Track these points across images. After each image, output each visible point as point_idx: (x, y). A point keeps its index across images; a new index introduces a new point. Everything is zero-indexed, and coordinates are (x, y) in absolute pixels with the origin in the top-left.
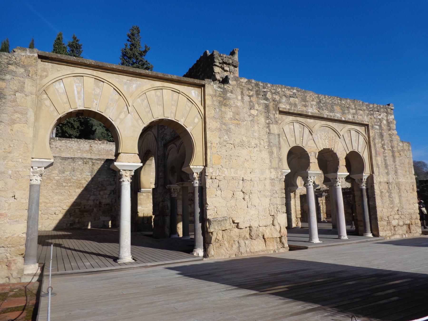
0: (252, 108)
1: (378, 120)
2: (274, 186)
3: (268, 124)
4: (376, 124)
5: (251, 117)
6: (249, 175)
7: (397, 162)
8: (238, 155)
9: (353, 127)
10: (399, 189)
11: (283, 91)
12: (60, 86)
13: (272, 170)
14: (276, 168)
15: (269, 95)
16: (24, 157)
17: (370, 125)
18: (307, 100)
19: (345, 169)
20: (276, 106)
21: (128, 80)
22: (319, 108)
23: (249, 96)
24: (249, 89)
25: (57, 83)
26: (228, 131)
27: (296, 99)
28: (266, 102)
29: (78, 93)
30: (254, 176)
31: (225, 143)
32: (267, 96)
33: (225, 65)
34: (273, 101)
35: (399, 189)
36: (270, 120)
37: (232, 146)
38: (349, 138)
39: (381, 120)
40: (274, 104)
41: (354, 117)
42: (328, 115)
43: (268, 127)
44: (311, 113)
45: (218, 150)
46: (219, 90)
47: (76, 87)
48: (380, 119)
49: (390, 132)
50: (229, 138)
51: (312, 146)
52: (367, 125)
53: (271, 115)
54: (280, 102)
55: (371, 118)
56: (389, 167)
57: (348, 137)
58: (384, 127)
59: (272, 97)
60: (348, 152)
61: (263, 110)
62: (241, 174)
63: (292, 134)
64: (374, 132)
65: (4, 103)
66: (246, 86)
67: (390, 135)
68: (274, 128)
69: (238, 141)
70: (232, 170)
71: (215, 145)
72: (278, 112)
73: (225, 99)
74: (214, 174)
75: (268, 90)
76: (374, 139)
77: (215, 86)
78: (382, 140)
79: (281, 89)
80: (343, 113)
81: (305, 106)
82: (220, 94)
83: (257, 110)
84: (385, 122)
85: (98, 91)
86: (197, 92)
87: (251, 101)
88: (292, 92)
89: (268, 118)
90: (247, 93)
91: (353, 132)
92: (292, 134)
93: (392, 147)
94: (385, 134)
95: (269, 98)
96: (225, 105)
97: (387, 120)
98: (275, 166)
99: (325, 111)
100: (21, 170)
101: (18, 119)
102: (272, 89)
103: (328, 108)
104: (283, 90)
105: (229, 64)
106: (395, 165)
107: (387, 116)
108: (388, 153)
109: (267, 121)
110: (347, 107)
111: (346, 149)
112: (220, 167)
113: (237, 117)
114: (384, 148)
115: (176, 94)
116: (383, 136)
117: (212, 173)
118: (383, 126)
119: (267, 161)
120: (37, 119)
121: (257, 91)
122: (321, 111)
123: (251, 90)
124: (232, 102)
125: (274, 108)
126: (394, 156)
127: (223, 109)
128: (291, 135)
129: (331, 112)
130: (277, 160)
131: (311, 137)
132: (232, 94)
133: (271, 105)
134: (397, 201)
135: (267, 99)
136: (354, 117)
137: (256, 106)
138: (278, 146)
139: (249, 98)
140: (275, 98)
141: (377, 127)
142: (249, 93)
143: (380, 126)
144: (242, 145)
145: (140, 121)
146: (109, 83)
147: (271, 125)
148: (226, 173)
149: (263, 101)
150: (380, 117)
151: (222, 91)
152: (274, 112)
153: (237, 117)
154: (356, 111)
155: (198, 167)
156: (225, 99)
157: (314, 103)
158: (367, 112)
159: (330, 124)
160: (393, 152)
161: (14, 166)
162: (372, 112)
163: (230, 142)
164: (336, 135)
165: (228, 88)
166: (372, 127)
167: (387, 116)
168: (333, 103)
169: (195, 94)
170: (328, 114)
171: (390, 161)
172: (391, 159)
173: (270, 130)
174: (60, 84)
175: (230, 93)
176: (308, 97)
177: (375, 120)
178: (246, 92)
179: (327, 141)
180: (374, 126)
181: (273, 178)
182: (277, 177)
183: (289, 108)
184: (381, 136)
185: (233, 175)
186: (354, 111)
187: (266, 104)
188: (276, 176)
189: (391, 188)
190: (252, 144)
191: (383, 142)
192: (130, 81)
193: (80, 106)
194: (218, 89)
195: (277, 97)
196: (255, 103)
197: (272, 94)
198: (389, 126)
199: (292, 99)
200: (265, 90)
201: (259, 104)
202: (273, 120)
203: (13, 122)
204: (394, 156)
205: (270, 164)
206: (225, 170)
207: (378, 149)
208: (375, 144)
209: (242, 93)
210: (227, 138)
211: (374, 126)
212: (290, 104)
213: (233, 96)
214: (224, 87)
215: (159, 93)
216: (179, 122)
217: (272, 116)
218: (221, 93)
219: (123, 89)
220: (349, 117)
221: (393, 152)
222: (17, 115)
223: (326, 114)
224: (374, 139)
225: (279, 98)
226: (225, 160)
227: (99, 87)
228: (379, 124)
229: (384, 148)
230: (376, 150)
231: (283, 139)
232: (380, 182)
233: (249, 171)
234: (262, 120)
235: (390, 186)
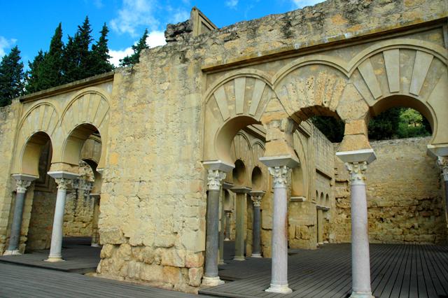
22: (288, 35)
23: (161, 67)
60: (372, 103)
87: (163, 73)
88: (229, 32)
104: (214, 36)
105: (182, 32)
111: (367, 96)
112: (117, 167)
123: (165, 58)
140: (199, 54)
152: (194, 75)
159: (320, 57)
164: (339, 74)
179: (310, 92)
182: (187, 174)
231: (213, 112)
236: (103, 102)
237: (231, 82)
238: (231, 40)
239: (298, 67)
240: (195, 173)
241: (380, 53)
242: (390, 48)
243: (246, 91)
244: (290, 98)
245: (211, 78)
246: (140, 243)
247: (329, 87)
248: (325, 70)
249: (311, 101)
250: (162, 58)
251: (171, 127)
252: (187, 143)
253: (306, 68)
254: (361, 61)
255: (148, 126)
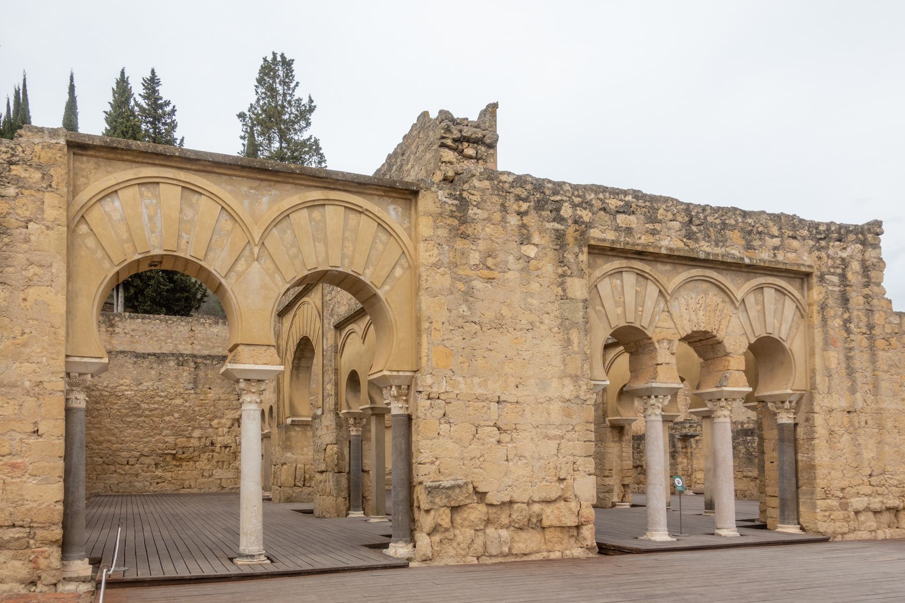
0: (525, 239)
1: (838, 262)
2: (569, 415)
3: (563, 275)
4: (832, 270)
5: (521, 261)
6: (514, 391)
7: (882, 364)
8: (490, 347)
9: (770, 280)
10: (881, 427)
11: (601, 200)
12: (113, 206)
13: (567, 381)
14: (577, 376)
15: (566, 211)
16: (52, 353)
17: (817, 273)
18: (659, 217)
19: (743, 378)
20: (583, 233)
21: (251, 188)
22: (690, 236)
23: (521, 214)
24: (518, 198)
25: (108, 199)
26: (469, 294)
27: (632, 218)
28: (557, 226)
29: (151, 218)
30: (525, 393)
31: (460, 322)
32: (562, 213)
33: (466, 144)
34: (576, 222)
35: (881, 427)
36: (566, 268)
37: (478, 327)
38: (759, 307)
39: (845, 263)
40: (576, 231)
41: (775, 255)
42: (708, 254)
43: (562, 284)
44: (667, 249)
45: (445, 337)
46: (450, 201)
47: (147, 207)
48: (843, 259)
49: (866, 291)
50: (469, 309)
51: (665, 325)
52: (808, 275)
53: (569, 256)
54: (589, 226)
55: (820, 258)
56: (857, 375)
57: (757, 304)
58: (853, 277)
59: (574, 215)
61: (551, 246)
62: (494, 388)
63: (617, 298)
64: (824, 290)
65: (7, 245)
66: (512, 190)
67: (866, 297)
68: (577, 288)
69: (490, 315)
70: (476, 380)
71: (438, 326)
72: (585, 249)
73: (463, 221)
74: (435, 390)
75: (565, 198)
76: (822, 309)
77: (440, 193)
78: (847, 309)
79: (596, 194)
80: (749, 247)
81: (654, 232)
82: (452, 211)
83: (537, 245)
84: (855, 266)
85: (189, 213)
86: (400, 209)
88: (621, 200)
89: (562, 262)
90: (515, 207)
91: (769, 293)
92: (617, 298)
93: (871, 327)
94: (854, 294)
95: (565, 216)
96: (464, 236)
97: (863, 262)
98: (573, 373)
99: (702, 243)
100: (46, 379)
101: (35, 278)
102: (573, 194)
103: (709, 237)
106: (874, 370)
107: (863, 252)
108: (860, 340)
109: (560, 271)
110: (760, 233)
112: (450, 373)
113: (490, 262)
114: (848, 331)
115: (353, 216)
116: (848, 300)
117: (430, 387)
118: (850, 275)
119: (557, 361)
120: (70, 277)
121: (539, 201)
122: (692, 244)
123: (525, 200)
124: (479, 227)
125: (576, 239)
126: (872, 348)
127: (459, 244)
128: (615, 301)
129: (717, 245)
130: (579, 358)
131: (662, 304)
132: (479, 211)
133: (571, 232)
134: (868, 454)
135: (560, 220)
136: (775, 255)
137: (536, 239)
138: (582, 327)
139: (519, 217)
140: (581, 217)
141: (835, 279)
142: (520, 207)
143: (843, 277)
144: (499, 325)
145: (278, 278)
146: (212, 196)
147: (569, 280)
148: (462, 386)
149: (552, 224)
150: (844, 255)
151: (456, 205)
152: (577, 250)
153: (490, 262)
154: (782, 241)
155: (401, 373)
156: (465, 222)
157: (677, 225)
158: (812, 243)
159: (714, 274)
160: (871, 338)
161: (34, 371)
162: (823, 243)
163: (472, 319)
165: (471, 197)
166: (822, 278)
167: (863, 252)
168: (724, 223)
169: (397, 213)
170: (708, 250)
171: (861, 360)
172: (866, 356)
173: (564, 290)
174: (113, 201)
175: (475, 209)
176: (661, 211)
177: (830, 262)
178: (513, 206)
180: (827, 277)
181: (567, 397)
183: (614, 238)
184: (845, 300)
185: (479, 391)
186: (776, 242)
187: (557, 230)
188: (575, 394)
189: (857, 424)
190: (523, 322)
191: (846, 316)
192: (255, 188)
193: (155, 247)
194: (447, 200)
195: (586, 215)
196: (532, 230)
197: (574, 206)
198: (868, 277)
199: (620, 218)
200: (558, 198)
201: (542, 231)
202: (575, 268)
203: (29, 283)
204: (872, 348)
205: (562, 367)
206: (460, 379)
207: (832, 332)
208: (824, 321)
209: (504, 208)
210: (466, 309)
211: (827, 277)
212: (617, 229)
213: (481, 214)
214: (461, 194)
215: (316, 214)
216: (362, 278)
217: (570, 257)
218: (454, 209)
219: (241, 207)
220: (764, 256)
221: (871, 338)
222: (33, 270)
223: (705, 248)
224: (823, 307)
225: (590, 214)
226: (461, 359)
227: (191, 206)
228: (839, 271)
229: (848, 331)
230: (826, 333)
231: (595, 310)
232: (831, 411)
233: (512, 382)
234: (549, 269)
235: (856, 420)
236: (383, 236)
237: (618, 275)
238: (624, 212)
239: (691, 280)
240: (588, 396)
241: (760, 288)
242: (770, 286)
243: (637, 292)
244: (682, 316)
245: (599, 261)
246: (507, 499)
247: (718, 313)
248: (714, 290)
249: (703, 325)
250: (518, 198)
251: (547, 321)
252: (574, 352)
253: (698, 283)
254: (748, 293)
255: (505, 311)
